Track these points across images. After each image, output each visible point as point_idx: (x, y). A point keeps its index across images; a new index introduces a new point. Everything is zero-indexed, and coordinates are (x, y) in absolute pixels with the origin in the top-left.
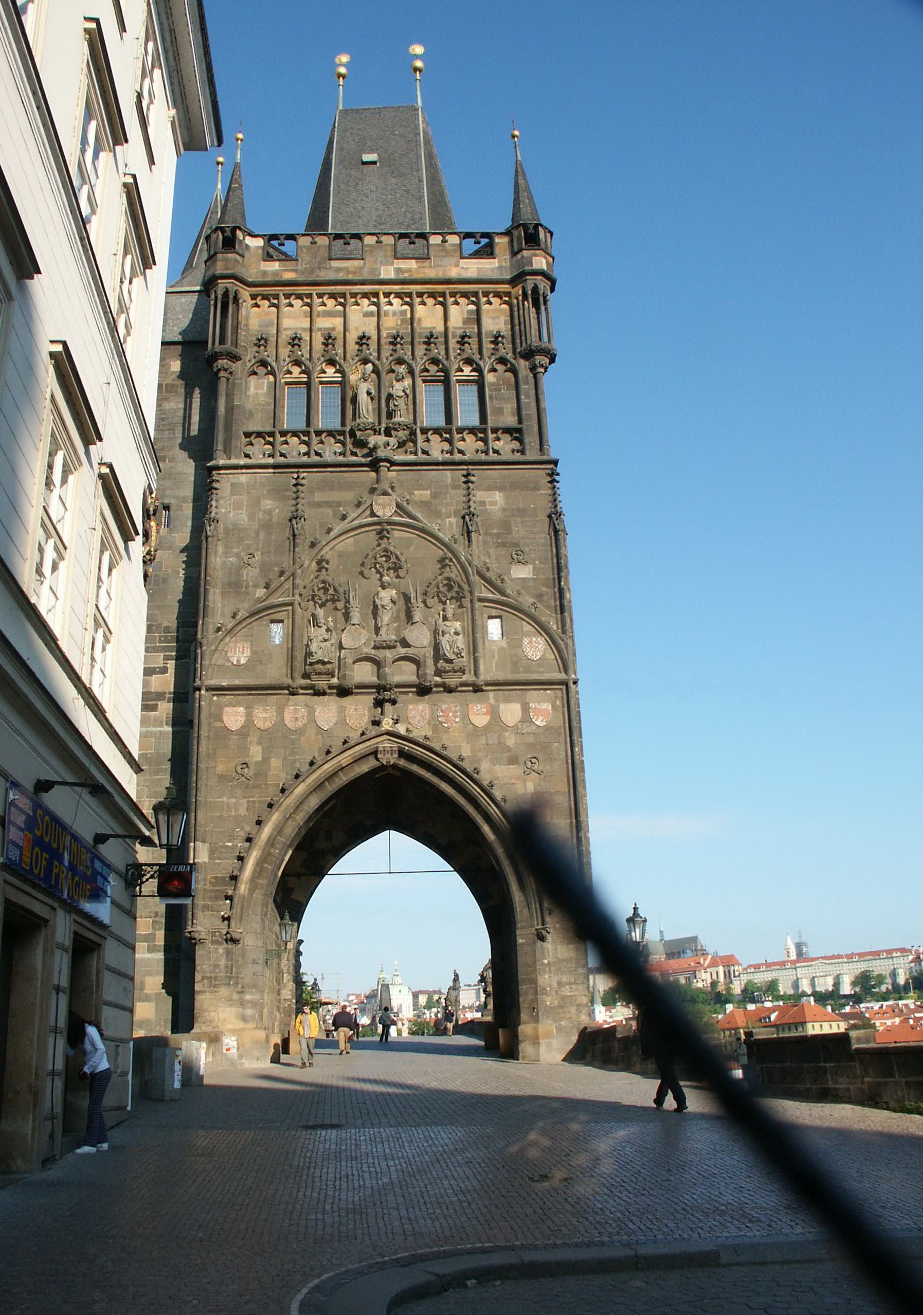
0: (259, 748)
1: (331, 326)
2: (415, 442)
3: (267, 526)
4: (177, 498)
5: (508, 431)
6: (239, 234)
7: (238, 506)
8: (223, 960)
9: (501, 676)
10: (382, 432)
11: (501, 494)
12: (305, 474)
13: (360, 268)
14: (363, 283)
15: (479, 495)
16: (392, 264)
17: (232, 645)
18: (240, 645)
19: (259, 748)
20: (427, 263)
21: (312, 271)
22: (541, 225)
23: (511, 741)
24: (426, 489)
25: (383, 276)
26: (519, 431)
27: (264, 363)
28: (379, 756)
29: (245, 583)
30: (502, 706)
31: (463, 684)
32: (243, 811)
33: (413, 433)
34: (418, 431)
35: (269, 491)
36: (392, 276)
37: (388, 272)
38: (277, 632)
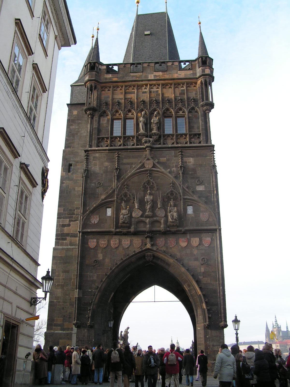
0: (102, 255)
1: (130, 97)
2: (160, 140)
3: (106, 172)
4: (75, 161)
5: (195, 135)
6: (97, 65)
7: (95, 165)
8: (86, 334)
9: (192, 228)
10: (149, 136)
11: (193, 159)
12: (120, 153)
13: (141, 76)
14: (142, 81)
15: (185, 159)
16: (153, 74)
17: (92, 216)
18: (95, 216)
19: (102, 255)
20: (166, 73)
21: (123, 77)
22: (208, 57)
23: (195, 252)
24: (164, 157)
25: (149, 78)
26: (199, 135)
27: (105, 112)
28: (146, 258)
29: (97, 193)
30: (192, 239)
31: (177, 231)
32: (95, 278)
33: (160, 137)
34: (162, 136)
35: (107, 159)
36: (153, 78)
37: (151, 77)
38: (109, 212)
